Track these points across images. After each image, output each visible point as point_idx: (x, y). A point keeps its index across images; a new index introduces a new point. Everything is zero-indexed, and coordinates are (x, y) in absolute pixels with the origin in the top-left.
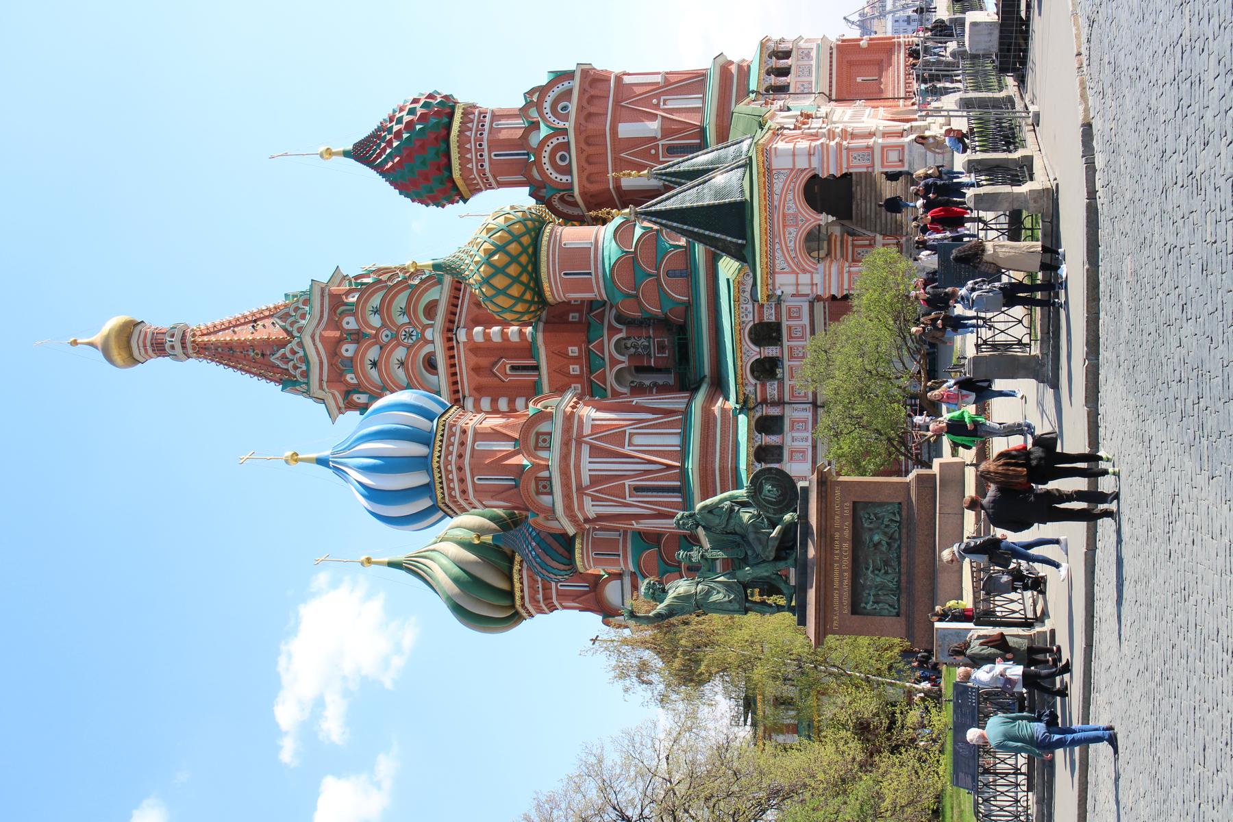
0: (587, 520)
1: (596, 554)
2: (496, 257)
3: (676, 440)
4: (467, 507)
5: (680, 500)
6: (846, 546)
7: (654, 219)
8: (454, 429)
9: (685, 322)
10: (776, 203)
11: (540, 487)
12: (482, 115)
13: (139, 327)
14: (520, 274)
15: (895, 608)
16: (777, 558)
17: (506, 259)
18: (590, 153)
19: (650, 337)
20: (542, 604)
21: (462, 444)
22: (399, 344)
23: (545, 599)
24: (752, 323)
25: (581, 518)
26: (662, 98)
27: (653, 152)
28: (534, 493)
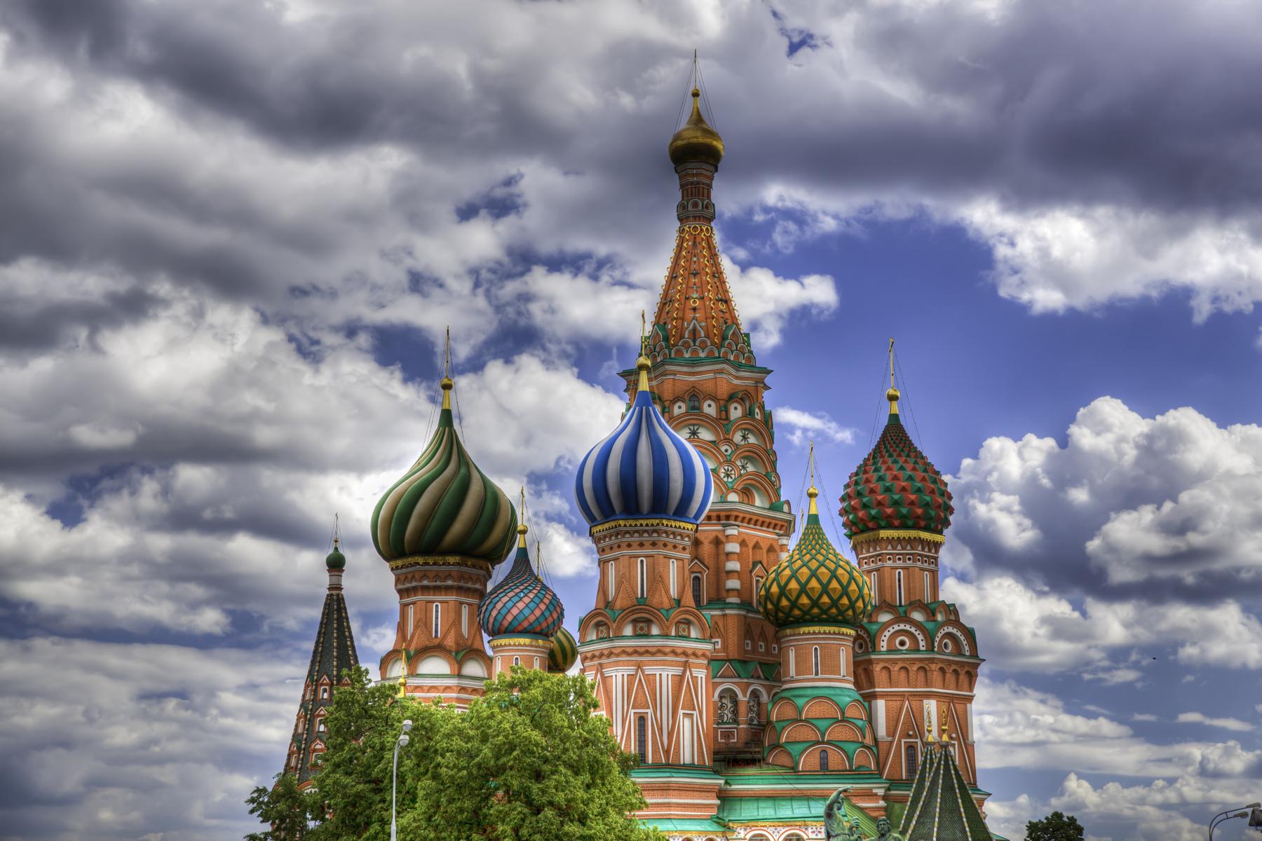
1: (517, 659)
2: (838, 586)
3: (688, 760)
4: (602, 544)
7: (942, 762)
8: (687, 539)
9: (768, 764)
13: (712, 168)
14: (819, 608)
17: (835, 597)
19: (738, 725)
22: (721, 464)
24: (805, 837)
25: (604, 661)
26: (956, 743)
27: (911, 733)
28: (635, 616)
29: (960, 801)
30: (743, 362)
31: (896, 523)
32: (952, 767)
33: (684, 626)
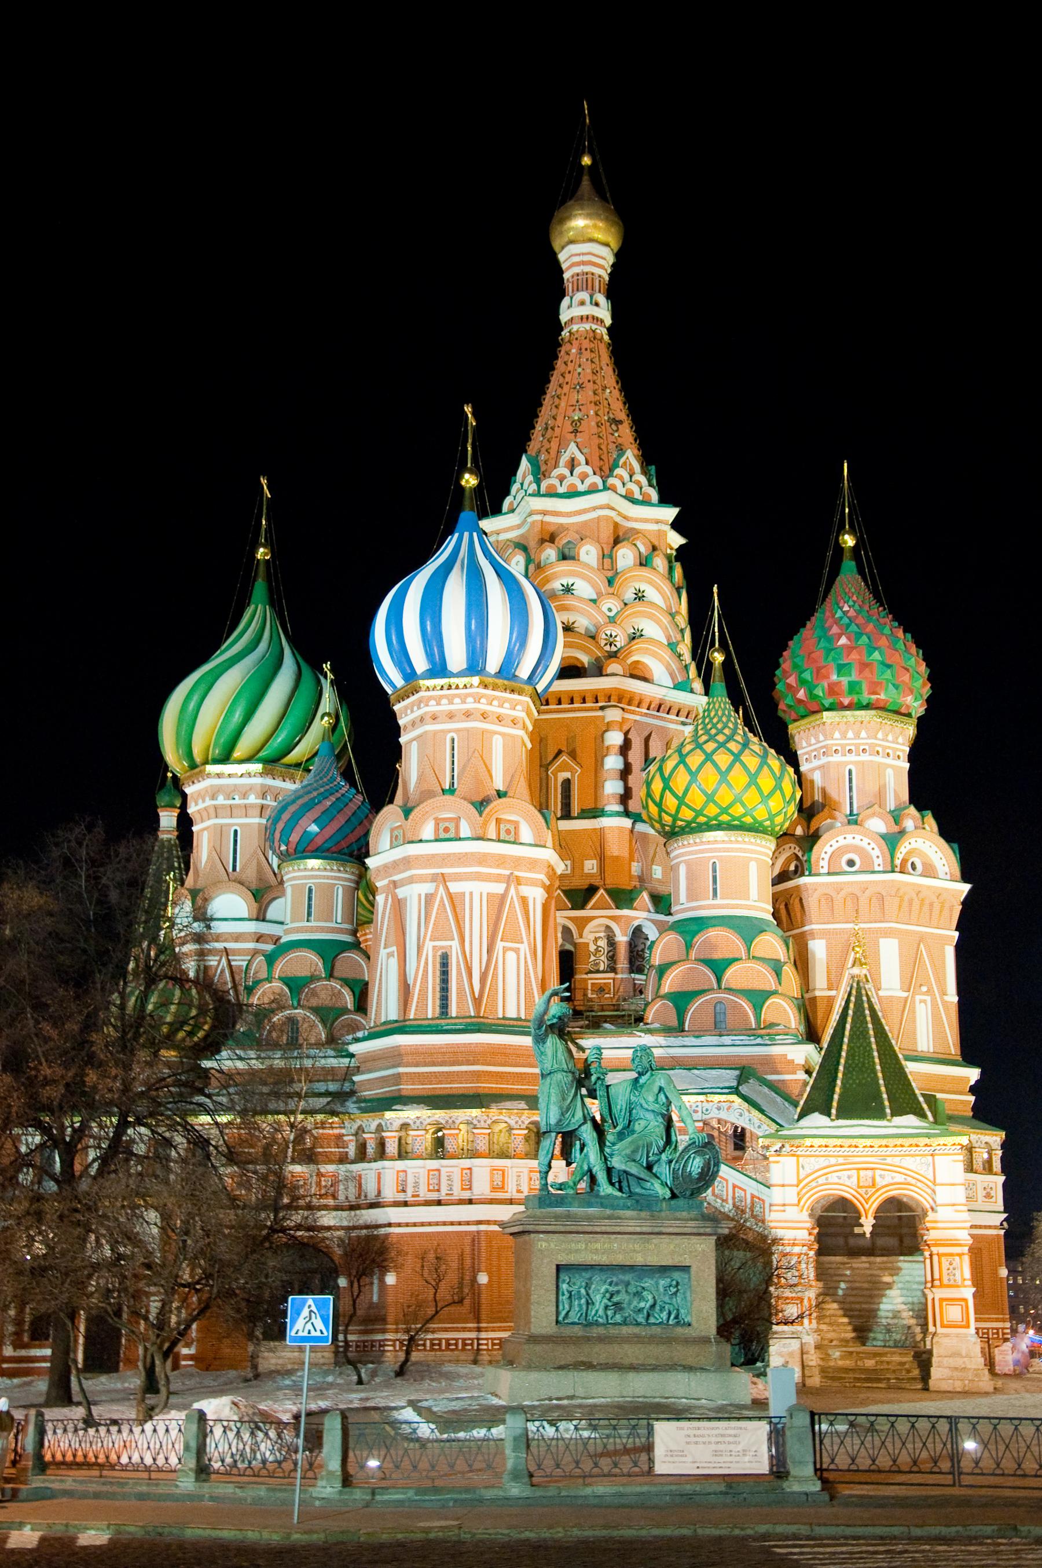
0: (395, 884)
3: (512, 1013)
5: (430, 1016)
6: (639, 1260)
7: (853, 999)
8: (519, 707)
10: (889, 1160)
11: (447, 824)
12: (901, 754)
15: (564, 1319)
16: (609, 1171)
18: (861, 900)
20: (209, 802)
21: (500, 719)
23: (216, 808)
26: (928, 998)
29: (876, 1054)
30: (640, 498)
31: (846, 702)
32: (866, 1005)
33: (508, 826)
